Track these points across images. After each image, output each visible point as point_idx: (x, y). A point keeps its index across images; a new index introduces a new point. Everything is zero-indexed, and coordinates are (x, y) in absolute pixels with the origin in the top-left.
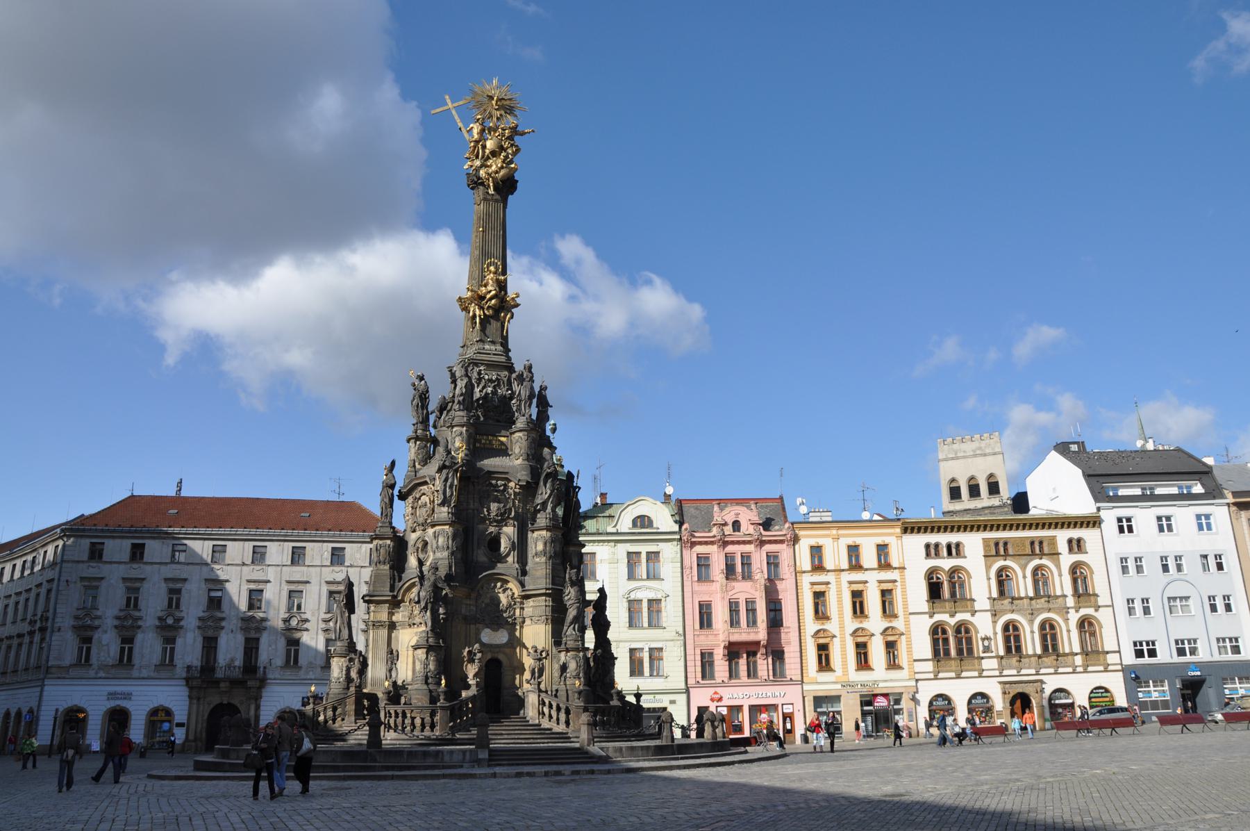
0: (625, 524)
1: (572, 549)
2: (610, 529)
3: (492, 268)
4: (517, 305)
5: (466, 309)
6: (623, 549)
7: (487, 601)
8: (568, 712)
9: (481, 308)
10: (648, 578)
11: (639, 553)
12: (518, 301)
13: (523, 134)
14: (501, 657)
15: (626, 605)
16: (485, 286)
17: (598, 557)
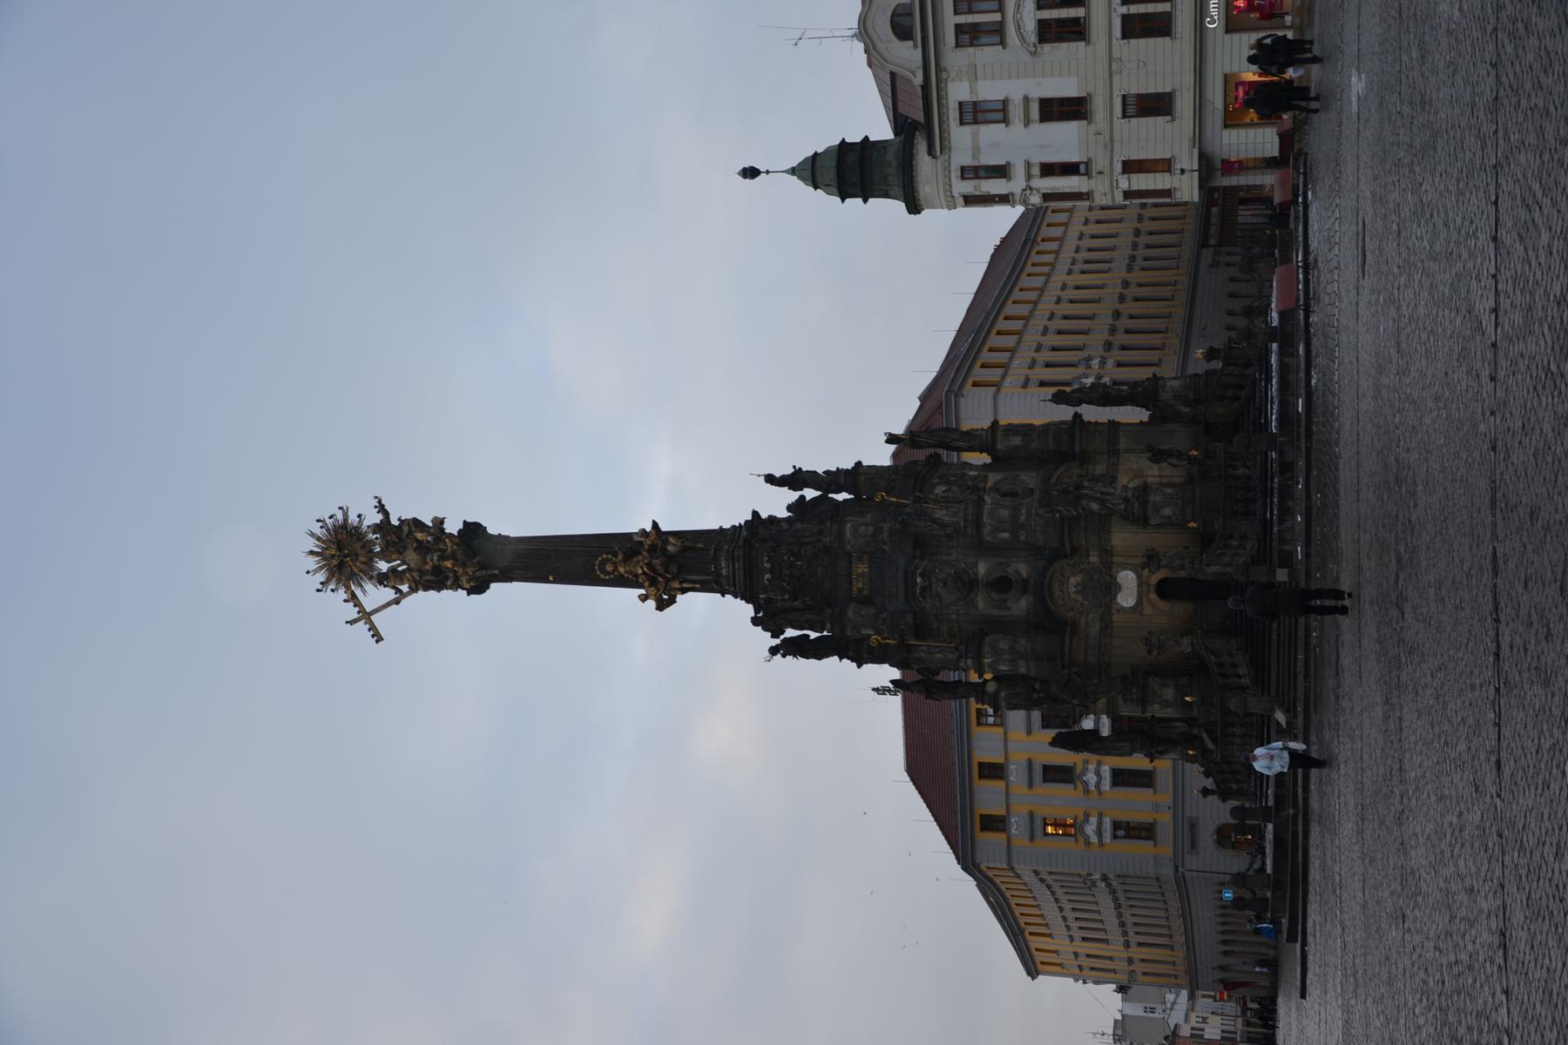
0: (907, 55)
1: (999, 446)
2: (918, 80)
3: (609, 568)
4: (655, 525)
5: (672, 601)
6: (956, 59)
7: (1079, 598)
8: (1231, 537)
9: (668, 581)
10: (1001, 9)
11: (958, 27)
12: (648, 529)
13: (386, 514)
14: (1154, 580)
15: (1047, 47)
16: (637, 576)
17: (966, 96)
